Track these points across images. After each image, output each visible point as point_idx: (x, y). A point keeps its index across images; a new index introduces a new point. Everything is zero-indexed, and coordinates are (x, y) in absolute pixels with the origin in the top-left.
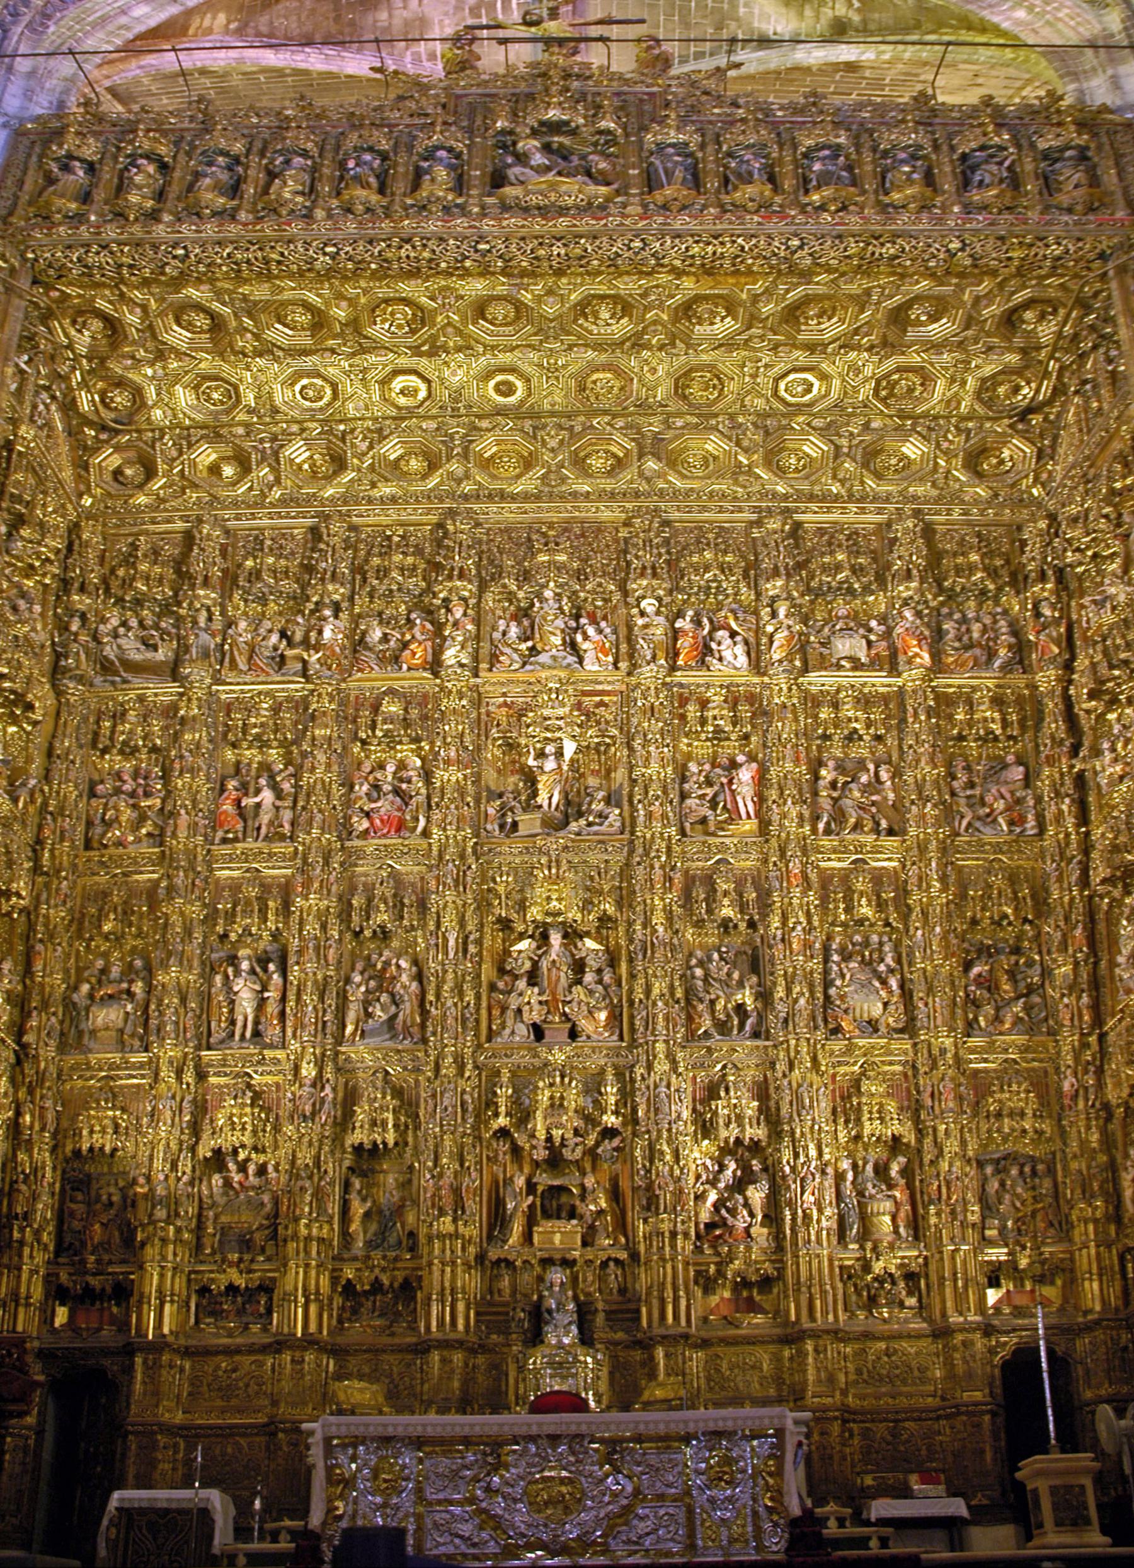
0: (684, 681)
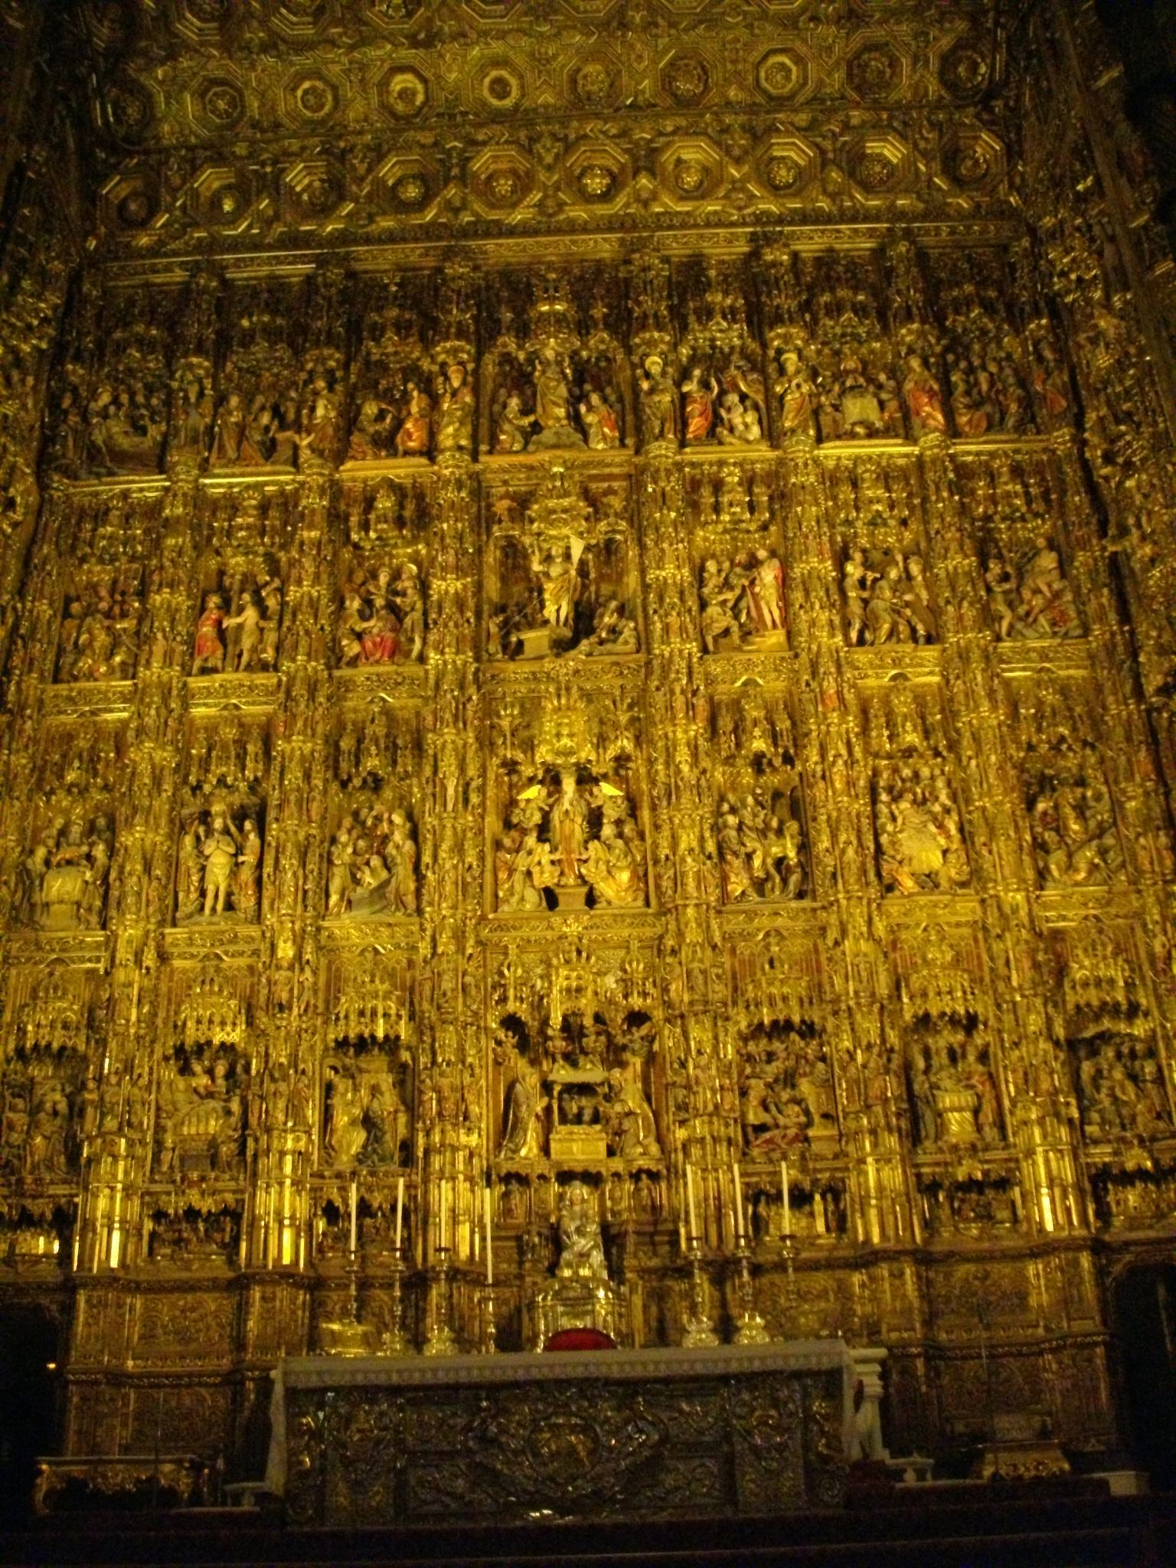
0: (695, 458)
